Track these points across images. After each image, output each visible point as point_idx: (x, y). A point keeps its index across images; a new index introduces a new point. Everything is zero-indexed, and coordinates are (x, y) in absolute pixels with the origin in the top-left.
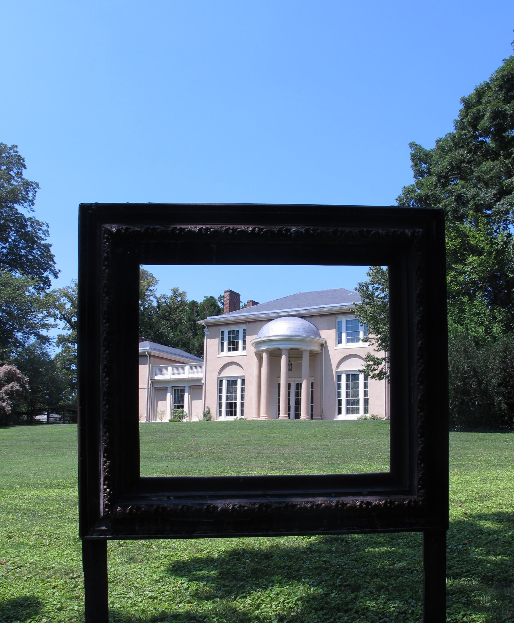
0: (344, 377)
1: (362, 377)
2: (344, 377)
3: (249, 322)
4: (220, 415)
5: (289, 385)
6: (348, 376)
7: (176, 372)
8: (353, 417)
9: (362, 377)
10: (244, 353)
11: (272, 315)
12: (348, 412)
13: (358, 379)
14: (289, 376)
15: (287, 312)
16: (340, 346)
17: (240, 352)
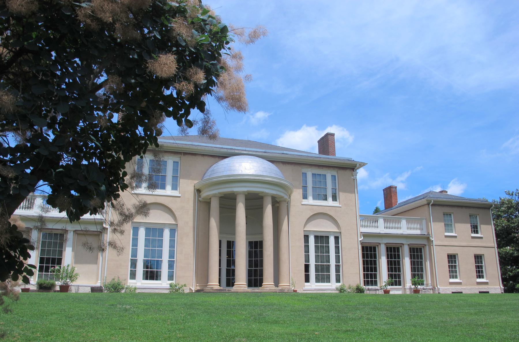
0: (312, 239)
1: (332, 240)
2: (312, 239)
3: (185, 154)
4: (133, 275)
5: (220, 242)
6: (316, 237)
7: (366, 223)
8: (323, 286)
9: (167, 233)
10: (176, 193)
11: (229, 151)
12: (318, 280)
13: (161, 235)
14: (221, 232)
15: (251, 151)
16: (305, 202)
17: (168, 191)
